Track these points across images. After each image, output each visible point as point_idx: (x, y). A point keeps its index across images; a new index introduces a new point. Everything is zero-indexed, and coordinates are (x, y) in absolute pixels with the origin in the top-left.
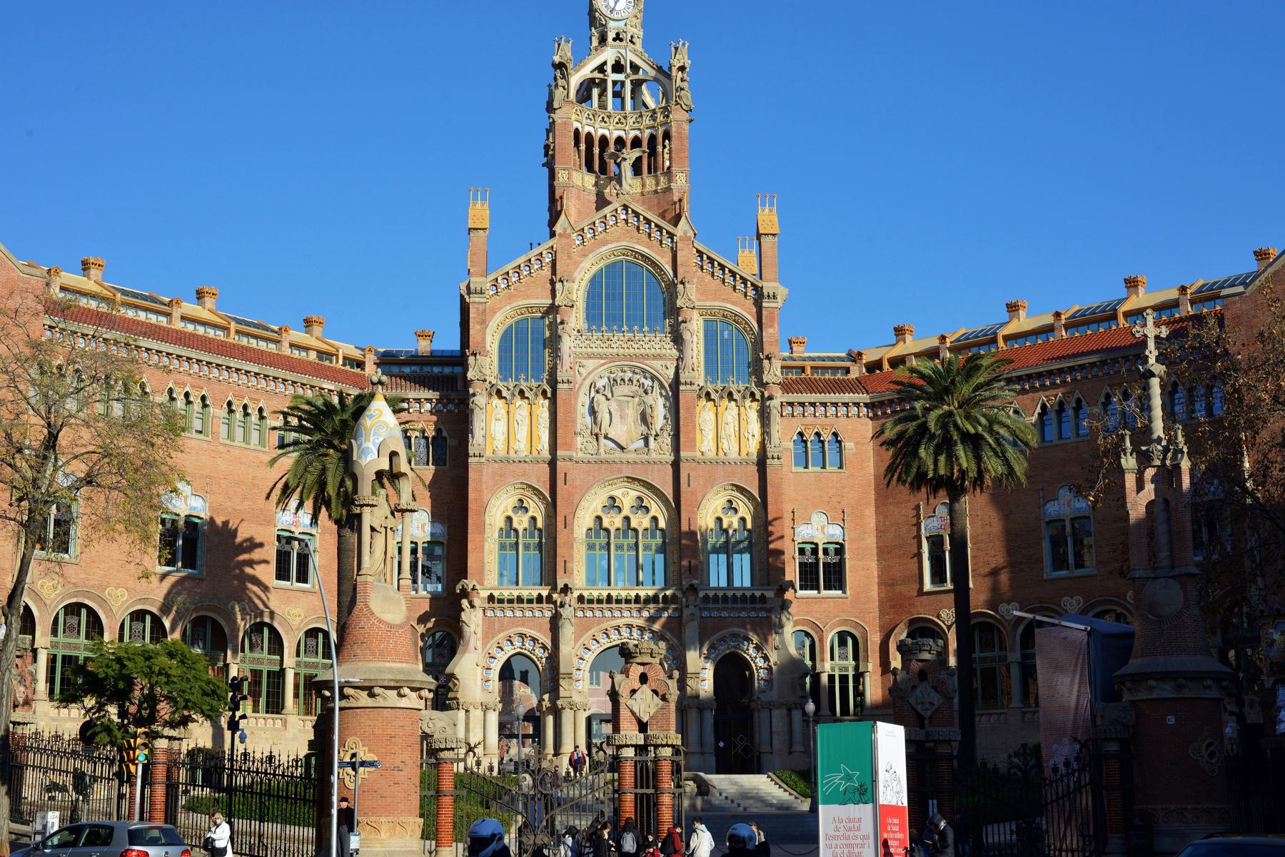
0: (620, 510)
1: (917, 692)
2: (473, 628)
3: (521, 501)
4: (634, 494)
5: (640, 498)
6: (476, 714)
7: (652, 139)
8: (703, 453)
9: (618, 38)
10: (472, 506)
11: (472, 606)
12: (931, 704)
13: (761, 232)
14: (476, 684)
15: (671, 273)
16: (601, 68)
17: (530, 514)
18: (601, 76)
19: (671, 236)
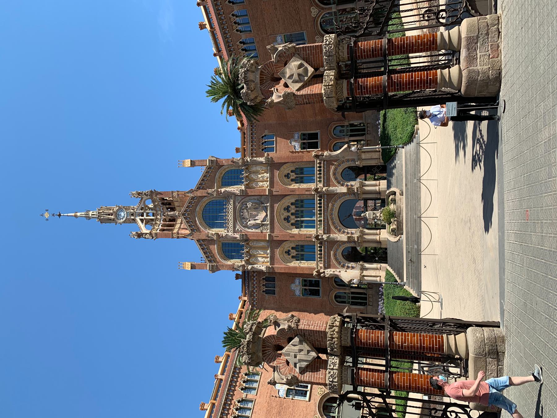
0: (288, 217)
1: (289, 82)
2: (332, 273)
3: (286, 252)
4: (282, 211)
5: (285, 209)
6: (365, 273)
7: (163, 204)
8: (268, 187)
9: (132, 215)
10: (287, 271)
11: (324, 272)
12: (300, 66)
13: (190, 165)
14: (352, 272)
15: (206, 197)
16: (142, 220)
17: (290, 249)
18: (144, 221)
19: (193, 198)
